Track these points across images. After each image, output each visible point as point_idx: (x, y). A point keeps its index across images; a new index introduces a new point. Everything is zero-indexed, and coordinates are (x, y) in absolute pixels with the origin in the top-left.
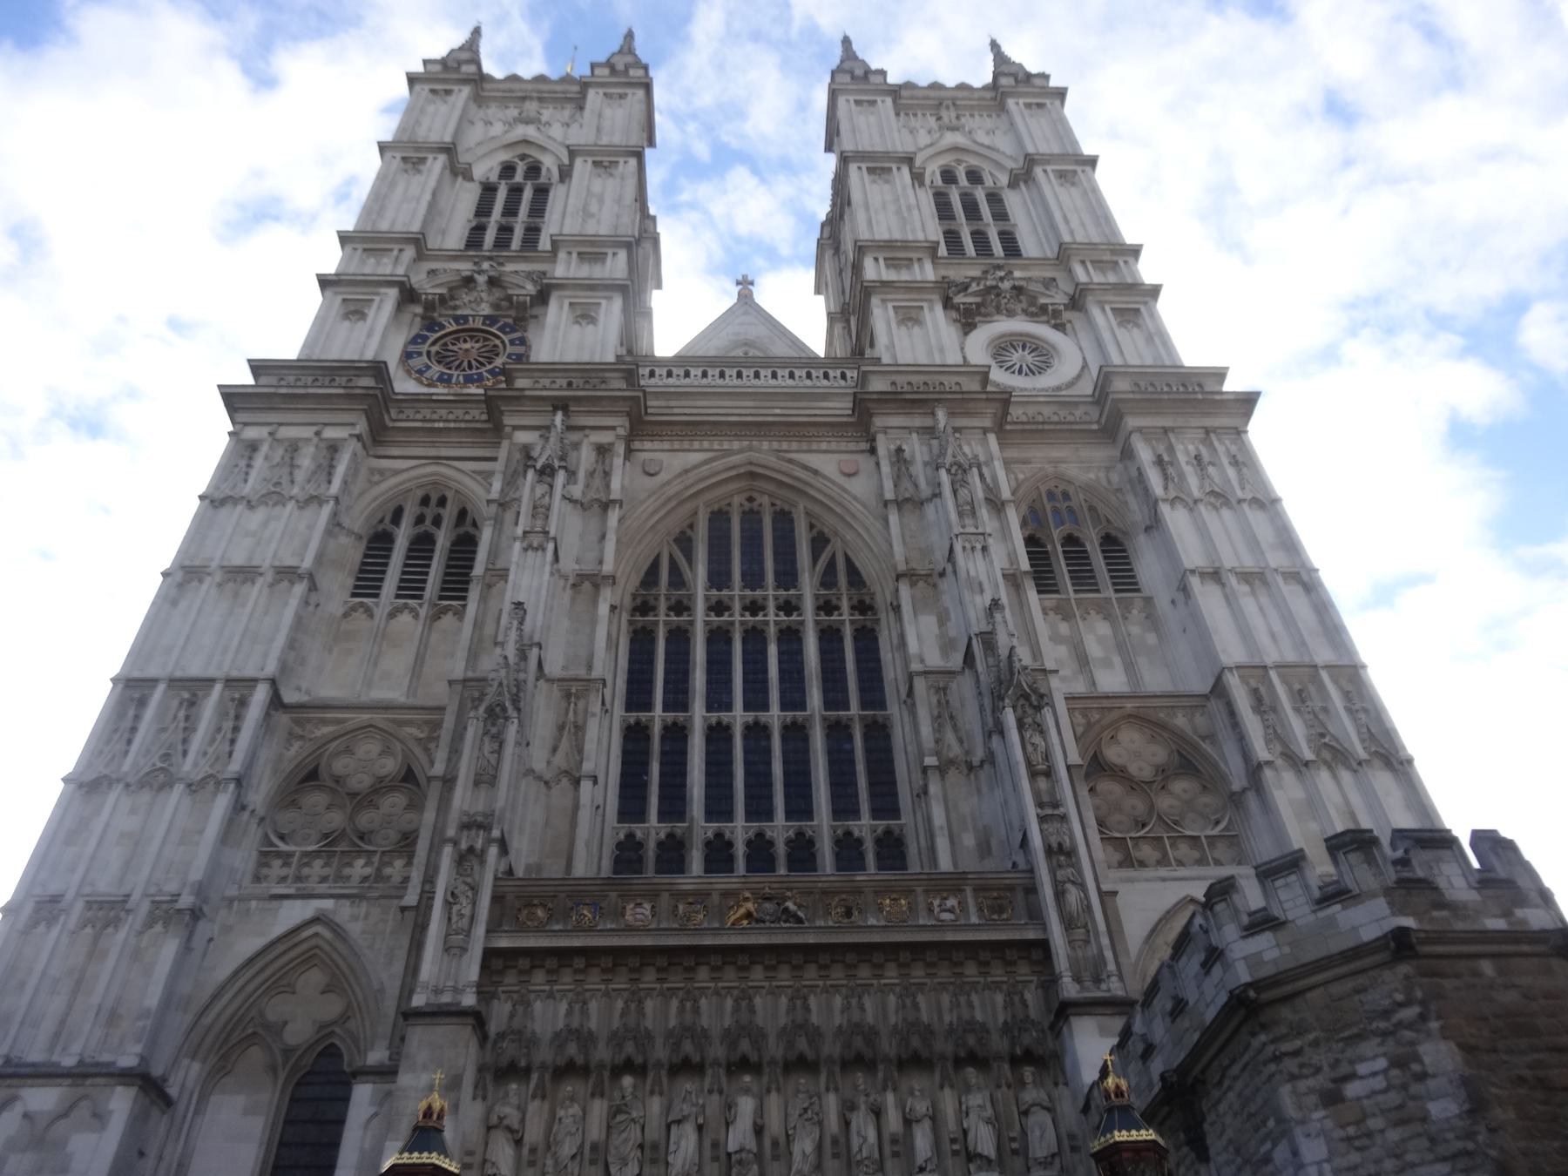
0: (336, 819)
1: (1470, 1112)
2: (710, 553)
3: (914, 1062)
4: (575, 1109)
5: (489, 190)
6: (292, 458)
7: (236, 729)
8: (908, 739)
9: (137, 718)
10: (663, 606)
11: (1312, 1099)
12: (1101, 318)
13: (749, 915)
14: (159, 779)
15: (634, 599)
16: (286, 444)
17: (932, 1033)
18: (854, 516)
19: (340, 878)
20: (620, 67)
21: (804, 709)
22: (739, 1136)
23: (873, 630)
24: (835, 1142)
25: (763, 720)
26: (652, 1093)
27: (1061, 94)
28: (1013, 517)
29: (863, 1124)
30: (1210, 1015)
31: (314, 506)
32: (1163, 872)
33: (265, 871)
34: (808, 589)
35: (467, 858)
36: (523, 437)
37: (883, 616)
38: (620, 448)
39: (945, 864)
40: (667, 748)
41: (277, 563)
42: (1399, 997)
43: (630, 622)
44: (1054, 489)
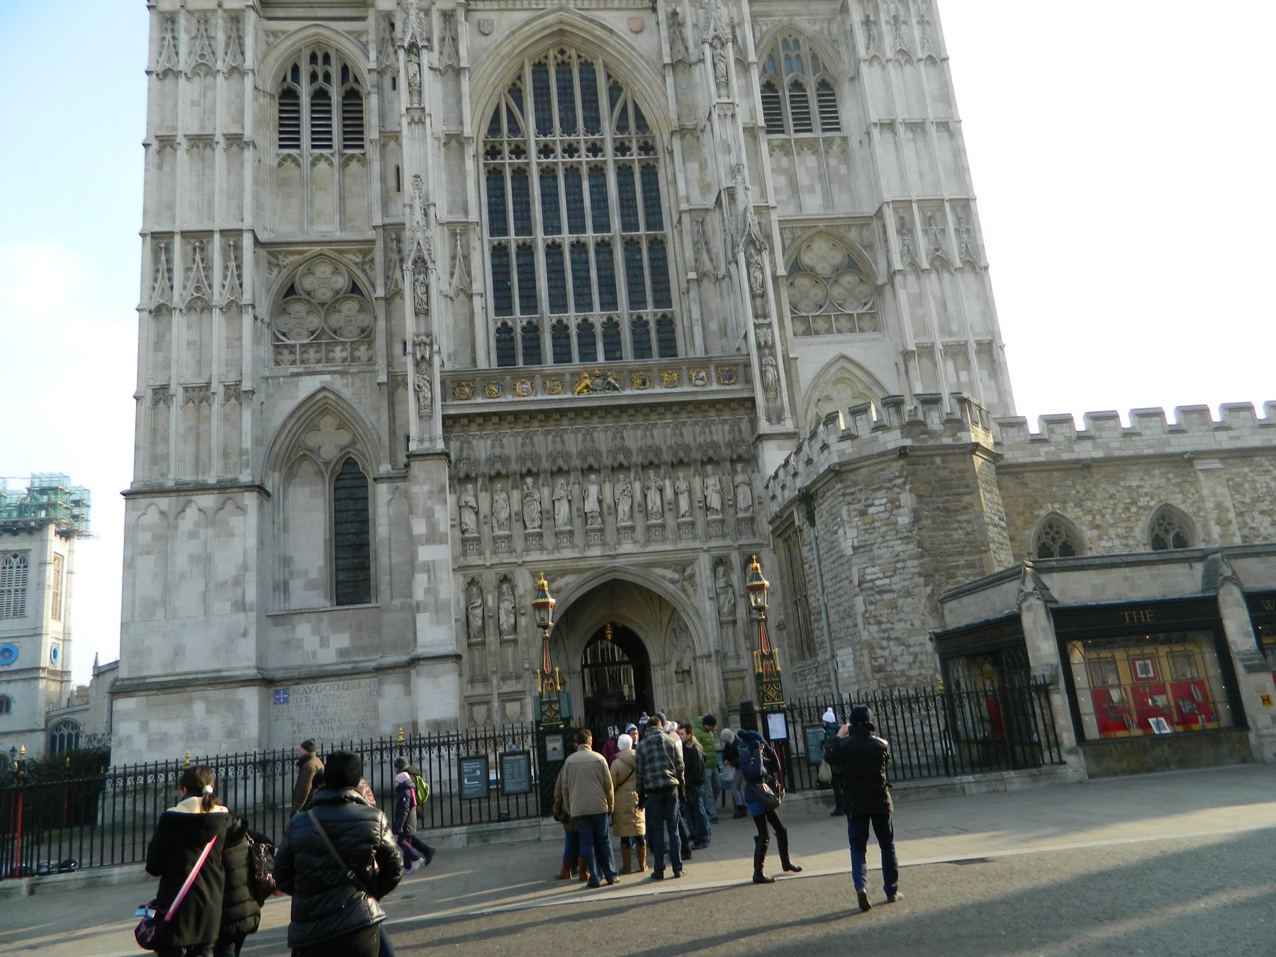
0: (314, 321)
1: (914, 522)
2: (536, 102)
3: (680, 463)
4: (504, 495)
6: (206, 30)
7: (239, 267)
8: (678, 253)
9: (169, 261)
11: (856, 513)
13: (587, 387)
14: (199, 305)
15: (485, 145)
16: (197, 15)
17: (690, 449)
18: (640, 72)
19: (328, 360)
21: (609, 231)
22: (591, 505)
23: (654, 167)
24: (639, 505)
25: (582, 240)
26: (543, 485)
28: (755, 74)
29: (654, 498)
30: (822, 470)
31: (236, 76)
32: (829, 338)
33: (280, 357)
35: (423, 363)
37: (660, 155)
38: (461, 14)
39: (699, 352)
40: (521, 262)
41: (226, 132)
42: (897, 474)
43: (485, 165)
44: (788, 37)
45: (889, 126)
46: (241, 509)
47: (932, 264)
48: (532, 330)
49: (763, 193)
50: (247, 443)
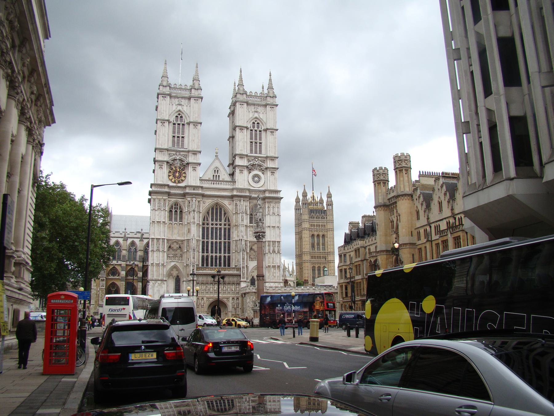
3: (229, 284)
5: (174, 124)
9: (154, 243)
10: (206, 224)
12: (269, 173)
14: (158, 250)
20: (196, 88)
27: (277, 105)
29: (225, 288)
34: (223, 222)
35: (193, 266)
36: (189, 199)
45: (269, 227)
46: (164, 284)
47: (272, 252)
48: (207, 256)
49: (247, 238)
50: (165, 274)
